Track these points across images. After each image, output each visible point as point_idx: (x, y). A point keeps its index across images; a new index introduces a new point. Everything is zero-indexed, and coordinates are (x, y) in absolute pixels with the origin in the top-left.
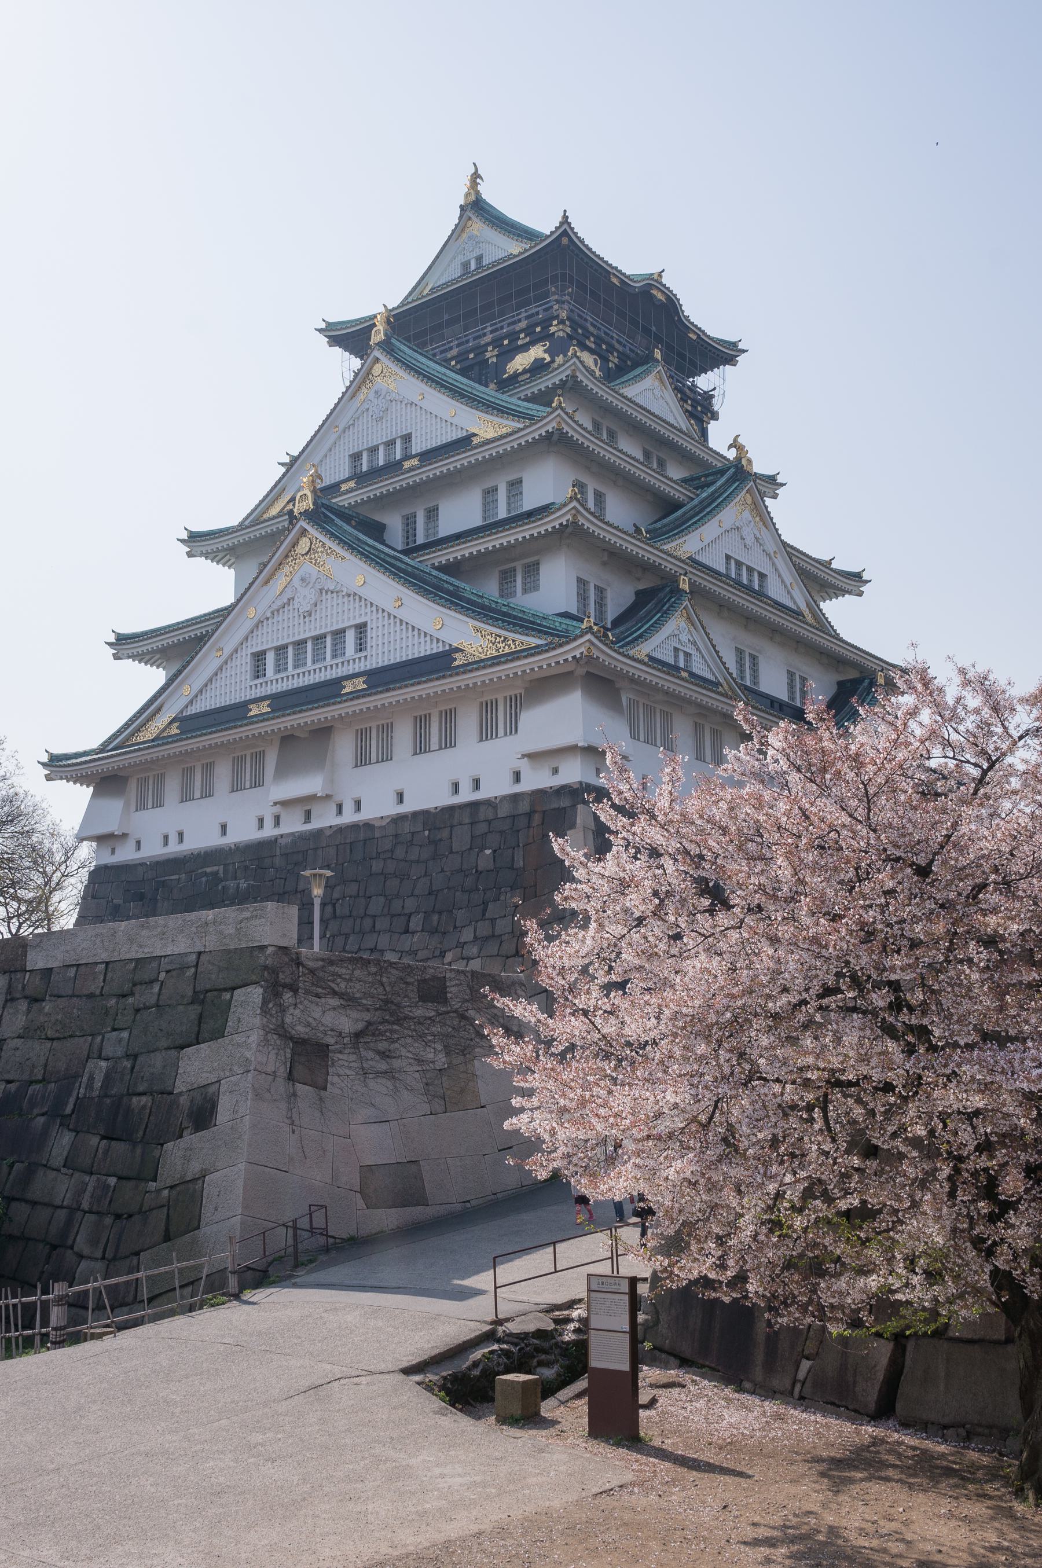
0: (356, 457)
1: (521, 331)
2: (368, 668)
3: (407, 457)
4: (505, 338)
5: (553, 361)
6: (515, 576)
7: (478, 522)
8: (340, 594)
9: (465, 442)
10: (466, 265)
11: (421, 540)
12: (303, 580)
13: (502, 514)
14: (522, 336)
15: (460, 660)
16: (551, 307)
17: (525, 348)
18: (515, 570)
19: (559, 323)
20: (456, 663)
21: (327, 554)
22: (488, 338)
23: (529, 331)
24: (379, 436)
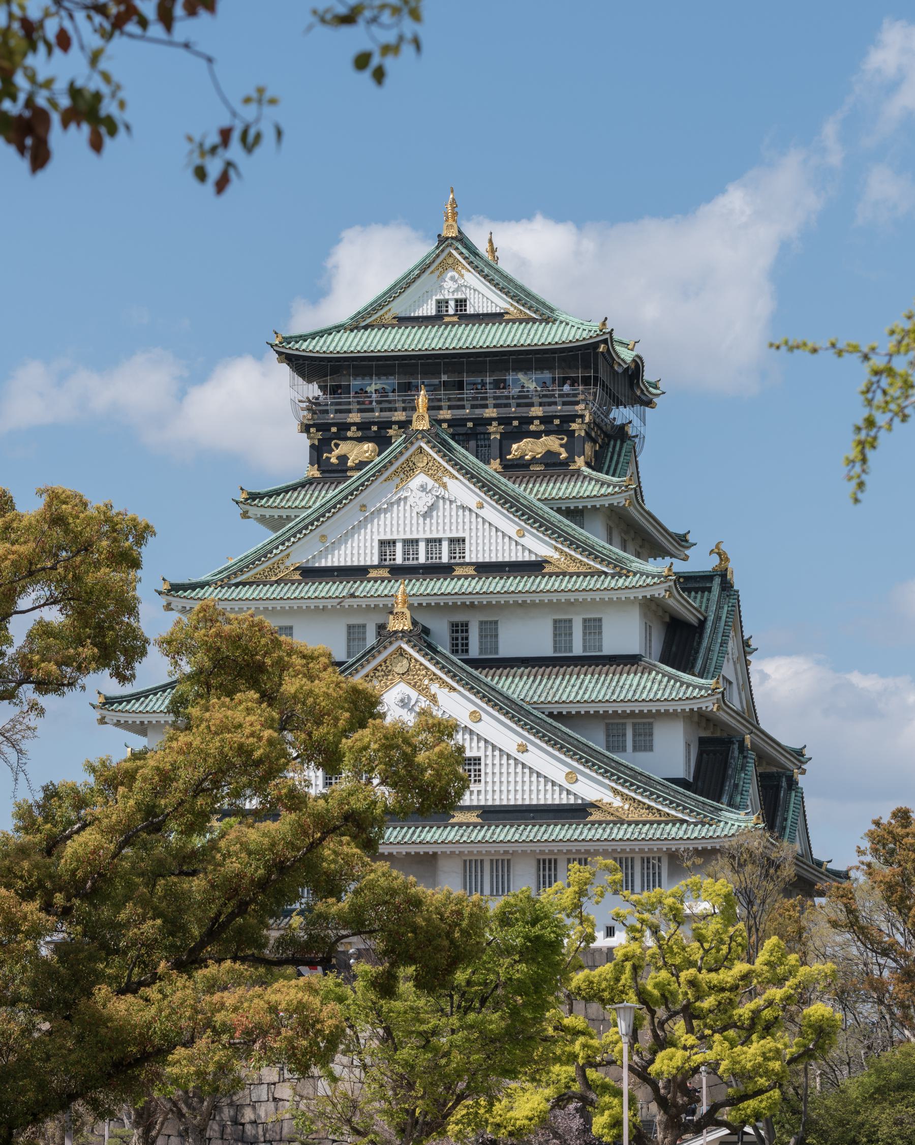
0: (386, 545)
2: (482, 803)
5: (571, 460)
7: (547, 650)
9: (535, 567)
10: (442, 304)
11: (474, 652)
13: (578, 650)
17: (537, 435)
18: (624, 724)
20: (590, 818)
22: (494, 415)
23: (546, 420)
24: (422, 532)
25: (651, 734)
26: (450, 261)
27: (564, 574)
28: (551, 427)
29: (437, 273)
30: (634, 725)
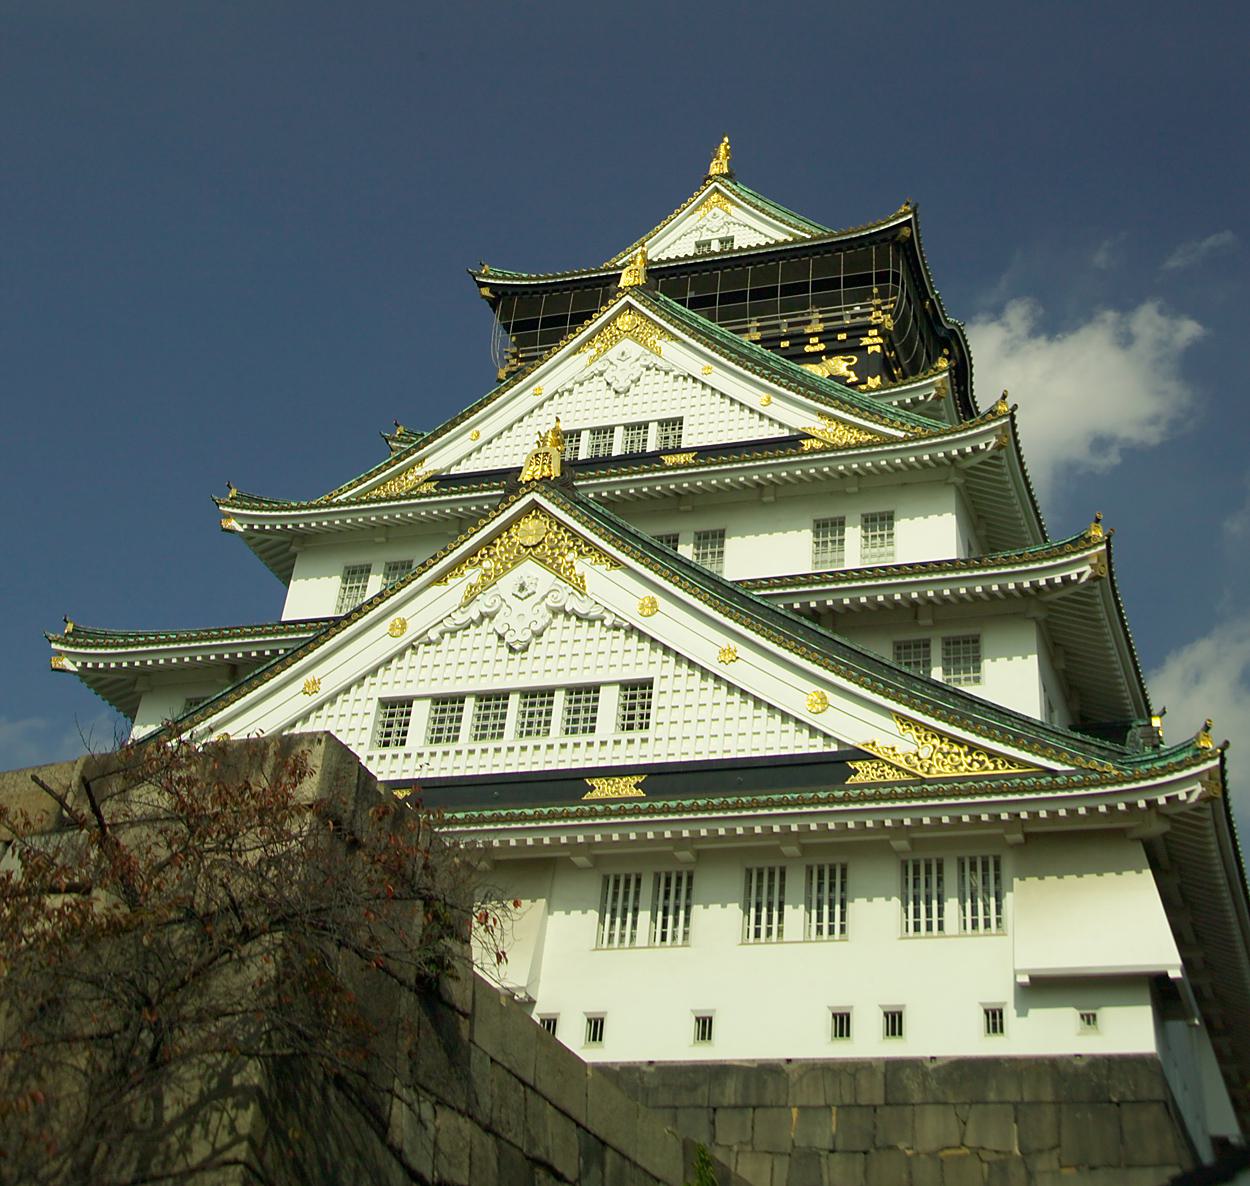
1: (813, 335)
3: (667, 452)
4: (785, 338)
6: (928, 654)
8: (598, 623)
12: (522, 588)
14: (815, 340)
15: (865, 773)
16: (870, 314)
17: (815, 358)
18: (927, 644)
19: (879, 335)
20: (852, 780)
21: (580, 553)
22: (757, 336)
23: (824, 336)
25: (977, 661)
26: (716, 195)
27: (835, 448)
28: (834, 346)
29: (698, 214)
30: (947, 642)
